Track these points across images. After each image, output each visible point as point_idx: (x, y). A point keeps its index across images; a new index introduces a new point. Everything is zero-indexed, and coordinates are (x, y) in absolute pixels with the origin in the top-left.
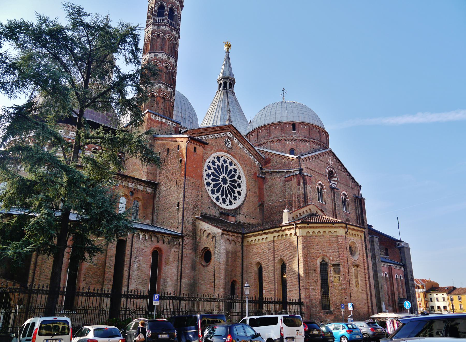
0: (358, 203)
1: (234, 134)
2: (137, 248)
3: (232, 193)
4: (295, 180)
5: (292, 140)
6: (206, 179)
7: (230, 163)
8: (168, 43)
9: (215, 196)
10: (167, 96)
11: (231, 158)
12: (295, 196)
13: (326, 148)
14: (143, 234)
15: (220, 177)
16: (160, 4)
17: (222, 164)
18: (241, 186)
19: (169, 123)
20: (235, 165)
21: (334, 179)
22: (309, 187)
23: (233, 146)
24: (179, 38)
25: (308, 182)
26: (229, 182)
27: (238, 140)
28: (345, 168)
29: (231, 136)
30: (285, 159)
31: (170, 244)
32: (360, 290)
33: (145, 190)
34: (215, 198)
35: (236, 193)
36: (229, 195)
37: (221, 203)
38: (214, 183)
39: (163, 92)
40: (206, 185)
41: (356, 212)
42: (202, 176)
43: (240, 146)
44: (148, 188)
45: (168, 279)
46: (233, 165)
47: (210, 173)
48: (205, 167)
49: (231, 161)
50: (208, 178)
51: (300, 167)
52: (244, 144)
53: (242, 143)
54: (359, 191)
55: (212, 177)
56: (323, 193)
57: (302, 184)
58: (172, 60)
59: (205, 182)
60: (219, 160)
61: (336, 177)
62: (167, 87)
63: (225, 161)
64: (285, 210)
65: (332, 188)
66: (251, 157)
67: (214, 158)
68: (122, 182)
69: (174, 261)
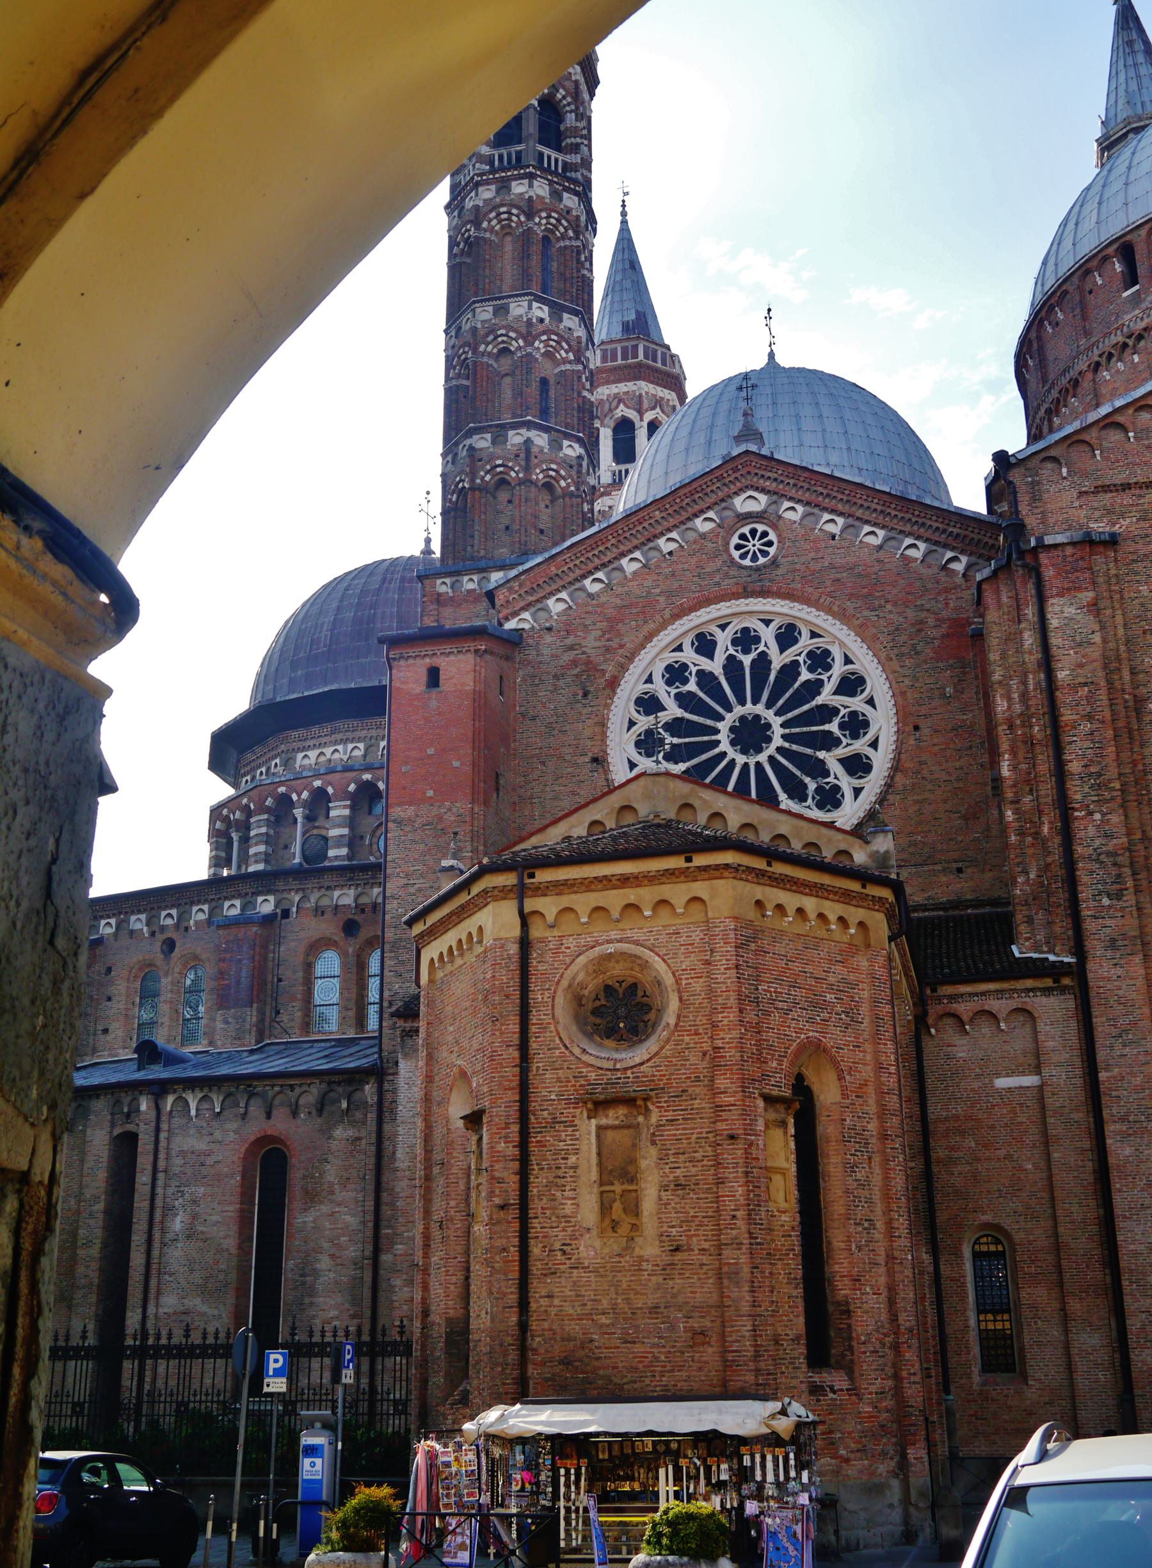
2: (183, 1153)
3: (807, 780)
10: (512, 469)
11: (777, 609)
14: (200, 1095)
15: (720, 725)
18: (866, 724)
27: (808, 504)
31: (325, 1114)
32: (649, 1248)
39: (488, 462)
43: (830, 528)
45: (319, 1261)
49: (788, 621)
52: (846, 508)
60: (706, 646)
63: (746, 639)
66: (912, 553)
69: (345, 1183)
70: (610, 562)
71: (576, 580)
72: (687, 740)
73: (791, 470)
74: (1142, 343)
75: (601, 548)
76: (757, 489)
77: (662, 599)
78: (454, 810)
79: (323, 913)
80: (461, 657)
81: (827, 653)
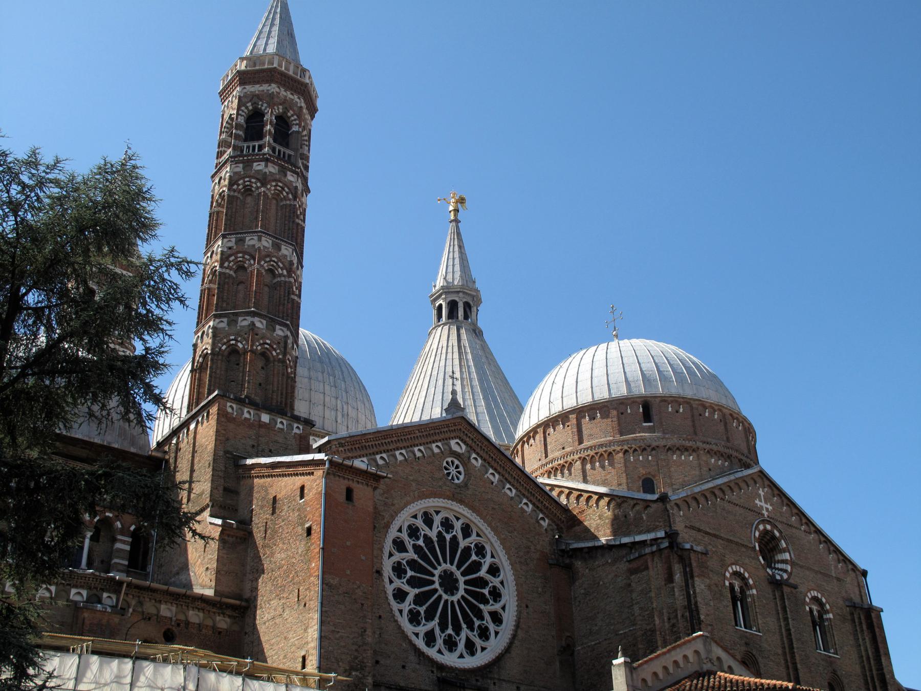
0: (861, 623)
1: (470, 442)
3: (475, 619)
4: (656, 570)
5: (644, 449)
6: (391, 582)
7: (462, 529)
8: (274, 207)
9: (422, 629)
10: (275, 350)
11: (465, 513)
12: (661, 614)
13: (747, 466)
16: (250, 108)
17: (439, 532)
19: (279, 426)
20: (478, 535)
21: (780, 557)
22: (700, 585)
23: (469, 479)
24: (307, 190)
25: (696, 571)
26: (462, 586)
27: (485, 460)
28: (809, 522)
29: (461, 449)
30: (625, 505)
33: (209, 622)
34: (421, 635)
35: (487, 616)
36: (464, 626)
37: (440, 652)
38: (417, 591)
39: (262, 338)
40: (391, 598)
41: (859, 652)
42: (379, 572)
43: (491, 477)
44: (218, 618)
46: (474, 534)
47: (404, 562)
48: (388, 545)
49: (468, 521)
50: (399, 577)
51: (670, 526)
52: (501, 470)
53: (495, 470)
54: (862, 589)
55: (410, 573)
56: (749, 600)
57: (678, 577)
58: (286, 251)
59: (390, 589)
60: (429, 522)
61: (784, 551)
62: (272, 324)
63: (447, 524)
64: (617, 658)
65: (776, 584)
66: (525, 507)
67: (415, 517)
68: (141, 603)
70: (391, 450)
71: (374, 454)
72: (419, 575)
73: (480, 437)
74: (654, 452)
75: (389, 440)
76: (462, 440)
77: (414, 484)
78: (362, 588)
79: (149, 619)
80: (366, 487)
81: (483, 548)
